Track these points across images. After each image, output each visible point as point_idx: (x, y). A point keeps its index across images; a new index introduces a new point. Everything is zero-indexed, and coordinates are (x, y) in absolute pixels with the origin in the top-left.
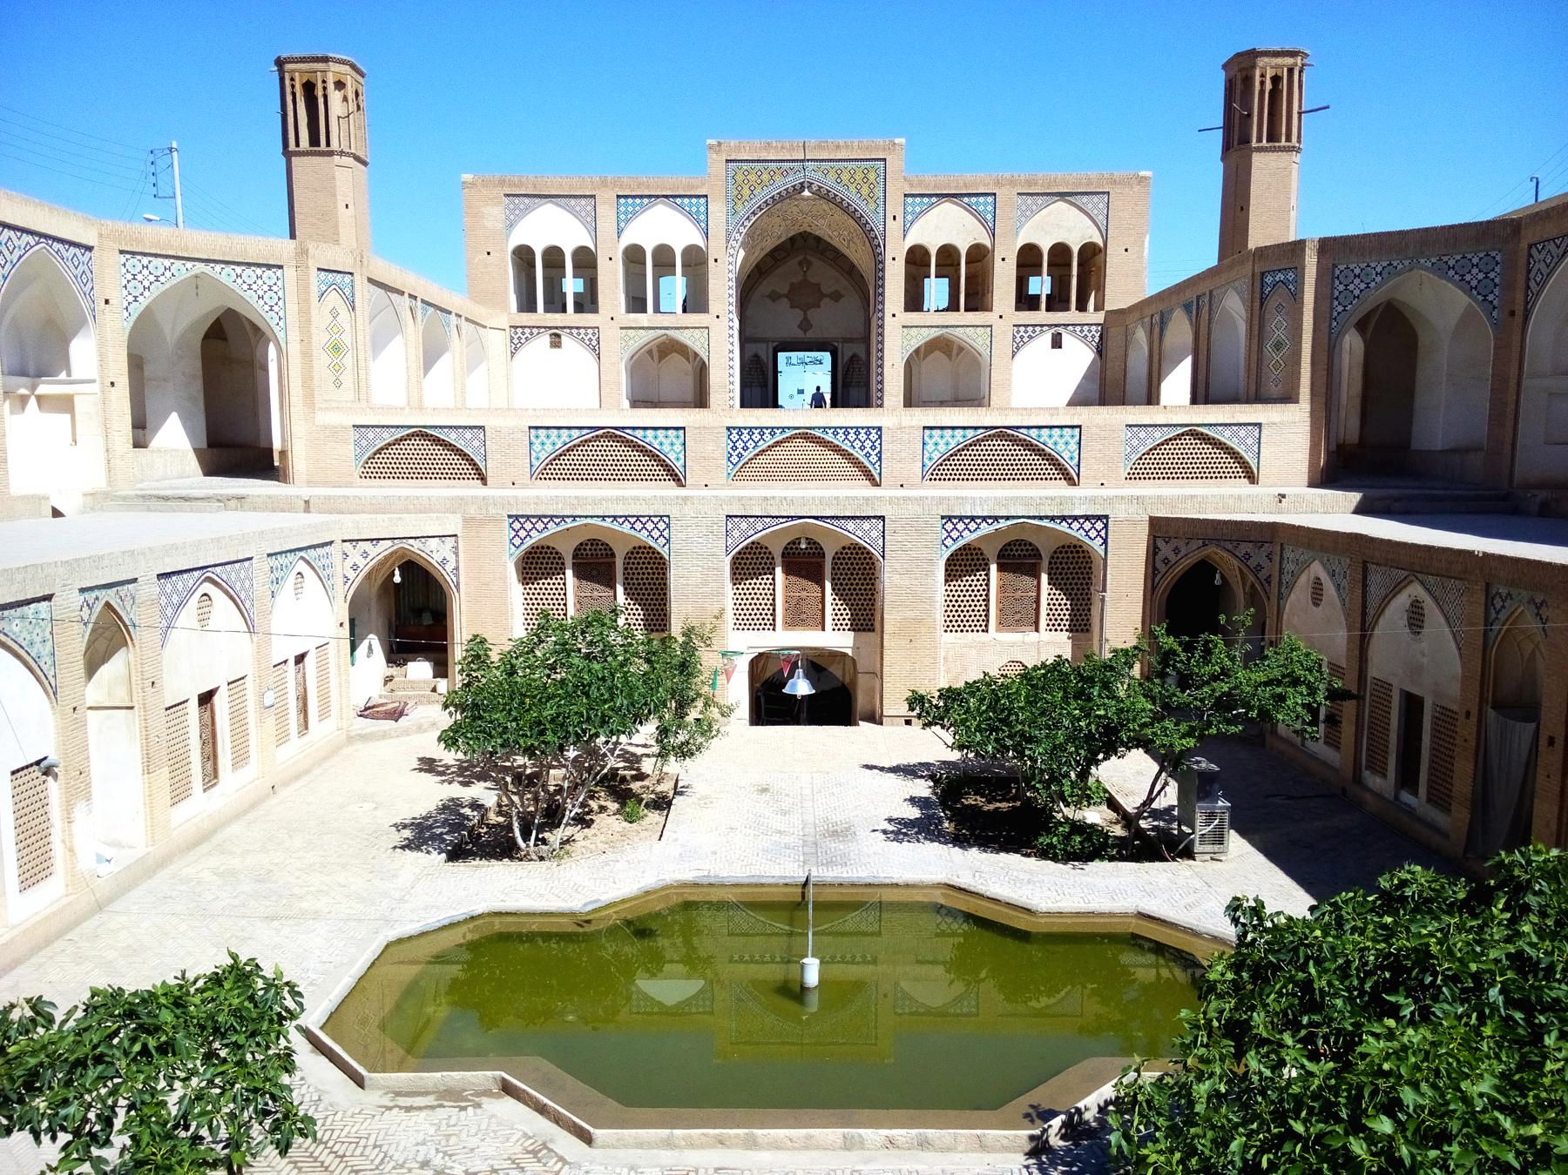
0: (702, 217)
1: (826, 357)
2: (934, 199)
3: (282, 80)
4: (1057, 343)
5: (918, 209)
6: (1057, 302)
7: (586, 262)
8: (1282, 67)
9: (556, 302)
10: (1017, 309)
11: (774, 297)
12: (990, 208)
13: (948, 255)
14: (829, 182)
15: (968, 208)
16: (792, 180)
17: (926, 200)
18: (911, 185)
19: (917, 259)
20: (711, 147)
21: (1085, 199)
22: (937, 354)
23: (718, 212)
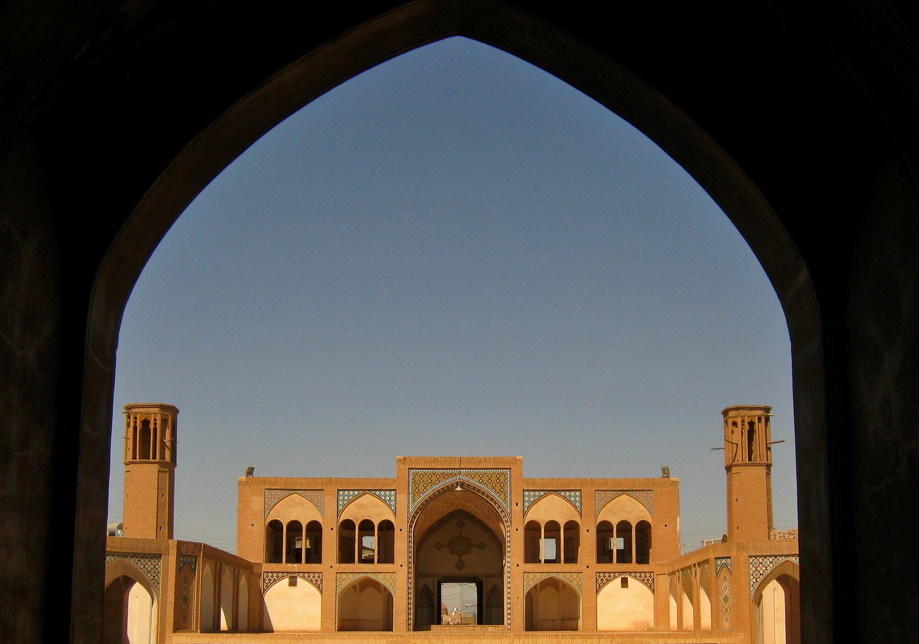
0: (392, 503)
1: (474, 585)
2: (542, 493)
3: (129, 417)
4: (624, 583)
5: (532, 499)
6: (624, 557)
7: (315, 529)
8: (754, 416)
9: (295, 556)
10: (599, 561)
11: (439, 546)
12: (578, 499)
13: (552, 529)
14: (475, 482)
15: (564, 497)
16: (450, 481)
17: (537, 494)
18: (527, 485)
19: (532, 530)
20: (399, 460)
21: (638, 494)
22: (549, 588)
23: (402, 499)
